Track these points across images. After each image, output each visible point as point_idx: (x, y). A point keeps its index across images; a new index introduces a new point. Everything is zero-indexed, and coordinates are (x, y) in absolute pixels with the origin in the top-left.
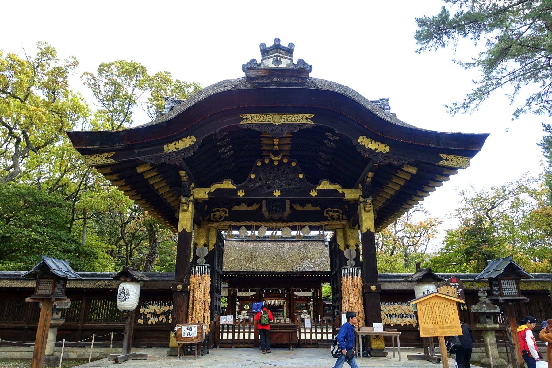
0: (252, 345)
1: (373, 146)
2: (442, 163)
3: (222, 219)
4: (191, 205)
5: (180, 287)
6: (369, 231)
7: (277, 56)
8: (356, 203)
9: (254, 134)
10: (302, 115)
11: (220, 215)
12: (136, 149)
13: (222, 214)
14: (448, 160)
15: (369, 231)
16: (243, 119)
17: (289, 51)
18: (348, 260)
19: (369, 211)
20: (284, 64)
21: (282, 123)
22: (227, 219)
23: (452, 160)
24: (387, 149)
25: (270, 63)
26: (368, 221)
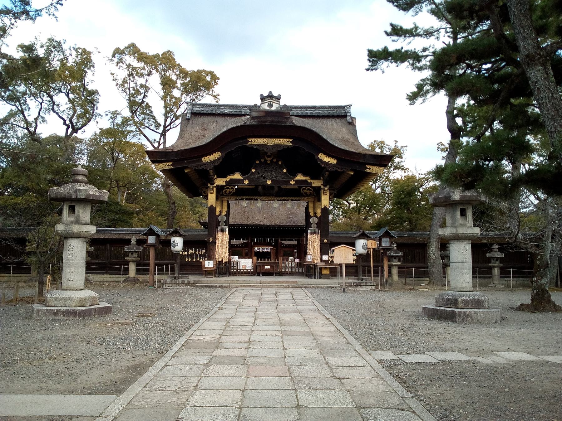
1: (327, 159)
2: (367, 170)
4: (215, 189)
5: (211, 239)
13: (231, 190)
17: (278, 98)
20: (275, 107)
24: (335, 161)
25: (265, 107)
26: (325, 200)
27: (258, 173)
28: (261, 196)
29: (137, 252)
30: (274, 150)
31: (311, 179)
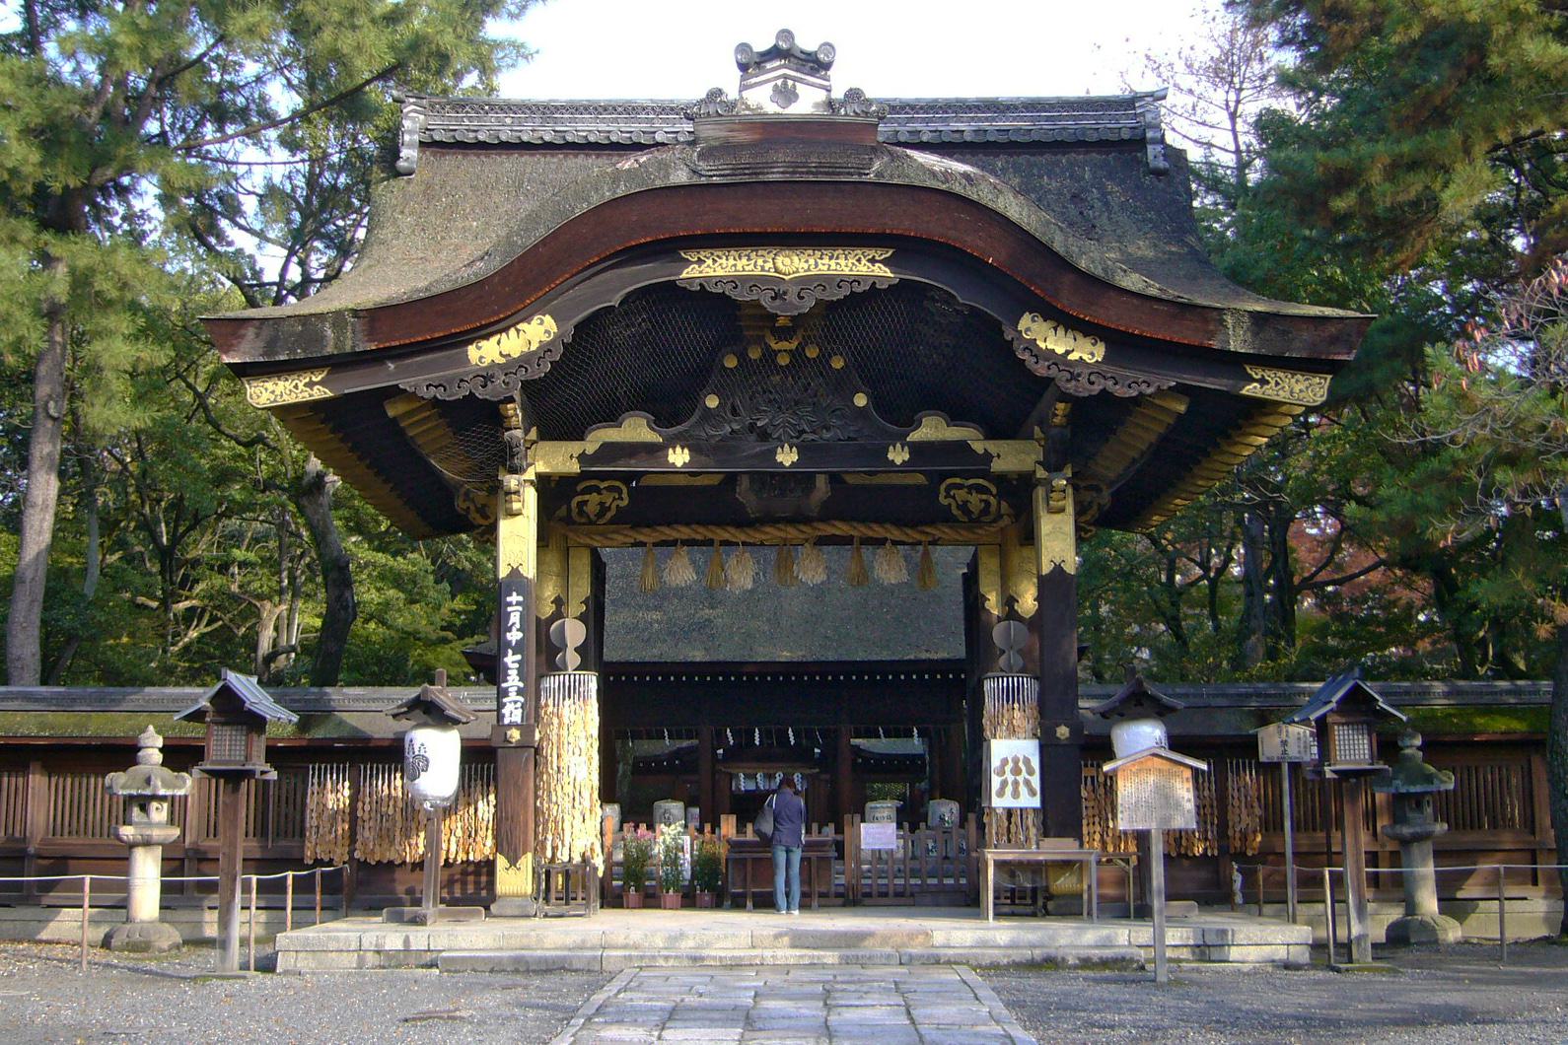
1: (1056, 342)
2: (1250, 390)
3: (609, 515)
4: (530, 496)
7: (786, 77)
11: (601, 504)
12: (392, 358)
14: (1268, 382)
16: (688, 263)
19: (1062, 510)
20: (808, 101)
22: (623, 518)
23: (1277, 384)
25: (762, 98)
29: (163, 798)
30: (809, 304)
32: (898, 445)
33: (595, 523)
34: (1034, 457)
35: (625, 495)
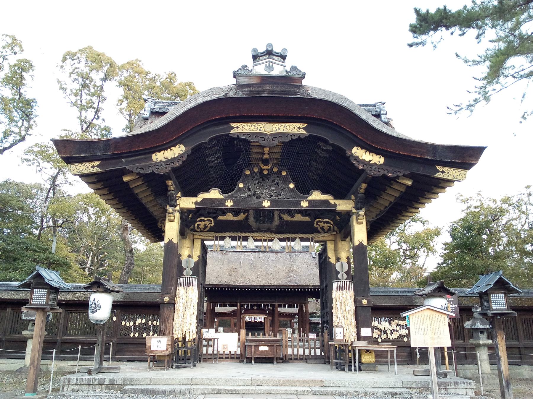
0: (238, 360)
4: (177, 215)
5: (167, 299)
6: (361, 244)
7: (269, 62)
8: (348, 215)
9: (244, 143)
10: (294, 125)
12: (124, 158)
13: (207, 223)
15: (361, 244)
16: (233, 128)
18: (339, 273)
19: (362, 223)
20: (278, 70)
21: (274, 132)
22: (211, 230)
25: (261, 70)
26: (360, 232)
27: (249, 189)
28: (253, 232)
30: (277, 142)
31: (335, 198)
32: (305, 201)
33: (202, 231)
34: (351, 206)
35: (213, 222)
